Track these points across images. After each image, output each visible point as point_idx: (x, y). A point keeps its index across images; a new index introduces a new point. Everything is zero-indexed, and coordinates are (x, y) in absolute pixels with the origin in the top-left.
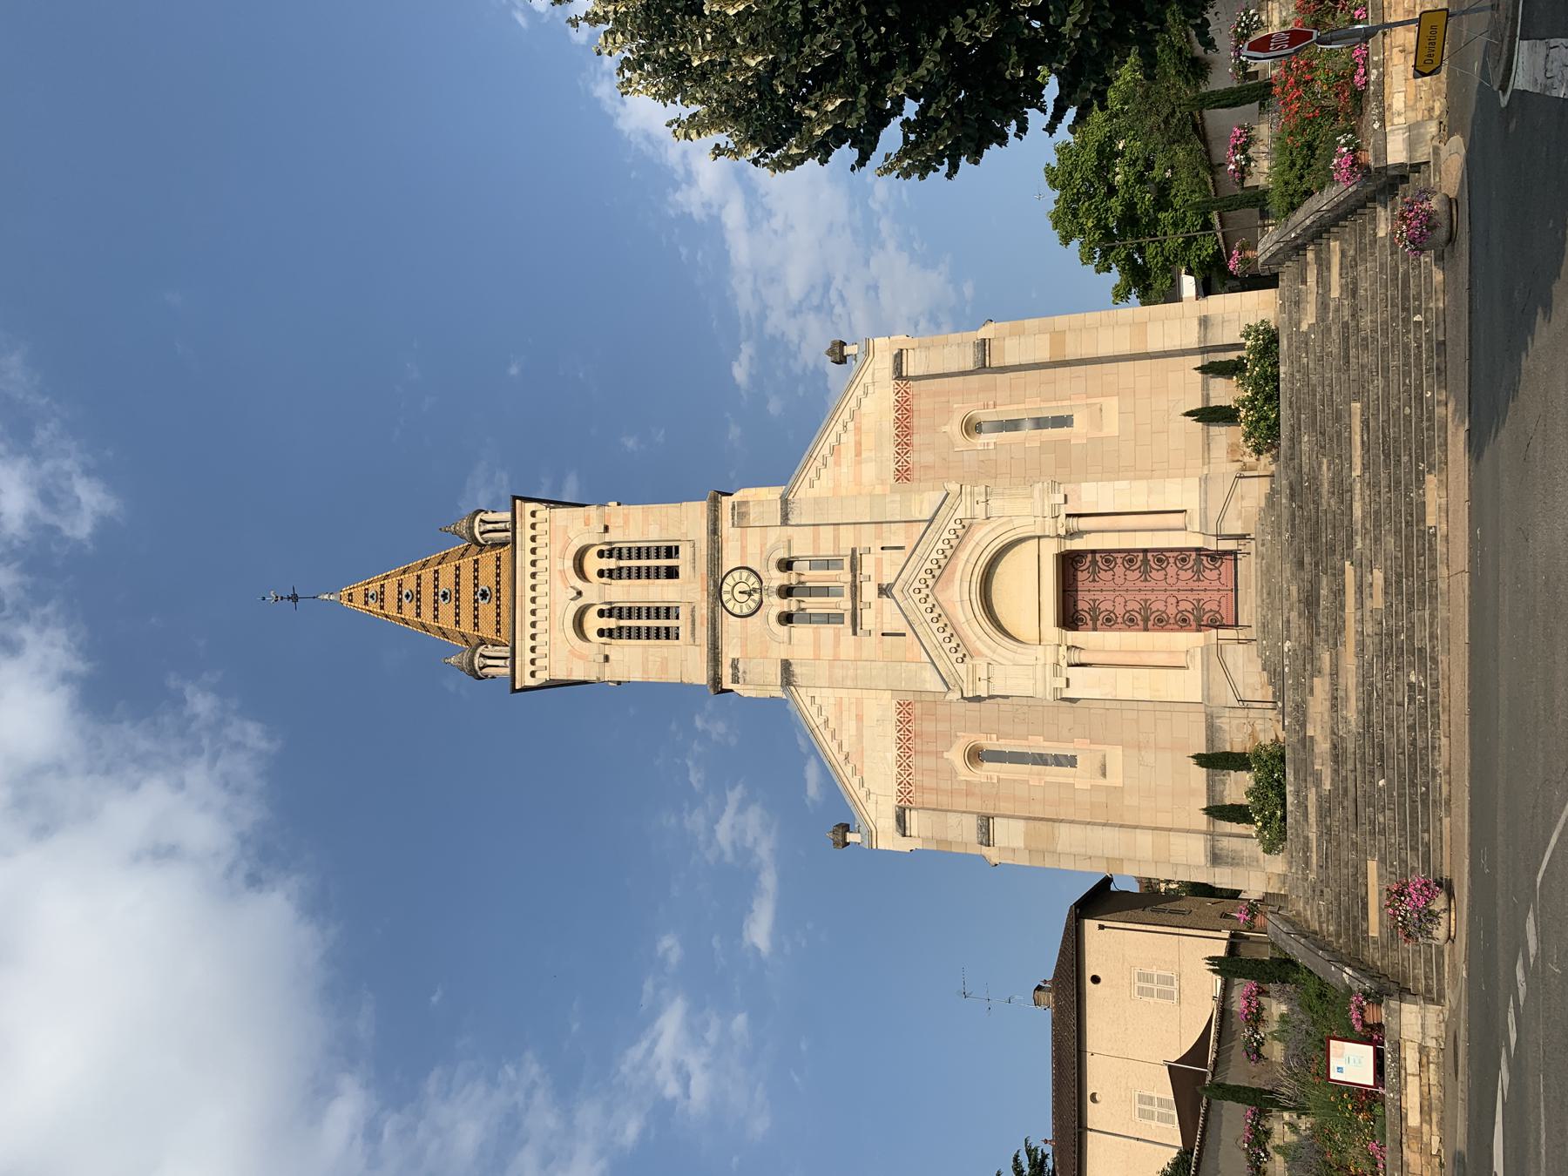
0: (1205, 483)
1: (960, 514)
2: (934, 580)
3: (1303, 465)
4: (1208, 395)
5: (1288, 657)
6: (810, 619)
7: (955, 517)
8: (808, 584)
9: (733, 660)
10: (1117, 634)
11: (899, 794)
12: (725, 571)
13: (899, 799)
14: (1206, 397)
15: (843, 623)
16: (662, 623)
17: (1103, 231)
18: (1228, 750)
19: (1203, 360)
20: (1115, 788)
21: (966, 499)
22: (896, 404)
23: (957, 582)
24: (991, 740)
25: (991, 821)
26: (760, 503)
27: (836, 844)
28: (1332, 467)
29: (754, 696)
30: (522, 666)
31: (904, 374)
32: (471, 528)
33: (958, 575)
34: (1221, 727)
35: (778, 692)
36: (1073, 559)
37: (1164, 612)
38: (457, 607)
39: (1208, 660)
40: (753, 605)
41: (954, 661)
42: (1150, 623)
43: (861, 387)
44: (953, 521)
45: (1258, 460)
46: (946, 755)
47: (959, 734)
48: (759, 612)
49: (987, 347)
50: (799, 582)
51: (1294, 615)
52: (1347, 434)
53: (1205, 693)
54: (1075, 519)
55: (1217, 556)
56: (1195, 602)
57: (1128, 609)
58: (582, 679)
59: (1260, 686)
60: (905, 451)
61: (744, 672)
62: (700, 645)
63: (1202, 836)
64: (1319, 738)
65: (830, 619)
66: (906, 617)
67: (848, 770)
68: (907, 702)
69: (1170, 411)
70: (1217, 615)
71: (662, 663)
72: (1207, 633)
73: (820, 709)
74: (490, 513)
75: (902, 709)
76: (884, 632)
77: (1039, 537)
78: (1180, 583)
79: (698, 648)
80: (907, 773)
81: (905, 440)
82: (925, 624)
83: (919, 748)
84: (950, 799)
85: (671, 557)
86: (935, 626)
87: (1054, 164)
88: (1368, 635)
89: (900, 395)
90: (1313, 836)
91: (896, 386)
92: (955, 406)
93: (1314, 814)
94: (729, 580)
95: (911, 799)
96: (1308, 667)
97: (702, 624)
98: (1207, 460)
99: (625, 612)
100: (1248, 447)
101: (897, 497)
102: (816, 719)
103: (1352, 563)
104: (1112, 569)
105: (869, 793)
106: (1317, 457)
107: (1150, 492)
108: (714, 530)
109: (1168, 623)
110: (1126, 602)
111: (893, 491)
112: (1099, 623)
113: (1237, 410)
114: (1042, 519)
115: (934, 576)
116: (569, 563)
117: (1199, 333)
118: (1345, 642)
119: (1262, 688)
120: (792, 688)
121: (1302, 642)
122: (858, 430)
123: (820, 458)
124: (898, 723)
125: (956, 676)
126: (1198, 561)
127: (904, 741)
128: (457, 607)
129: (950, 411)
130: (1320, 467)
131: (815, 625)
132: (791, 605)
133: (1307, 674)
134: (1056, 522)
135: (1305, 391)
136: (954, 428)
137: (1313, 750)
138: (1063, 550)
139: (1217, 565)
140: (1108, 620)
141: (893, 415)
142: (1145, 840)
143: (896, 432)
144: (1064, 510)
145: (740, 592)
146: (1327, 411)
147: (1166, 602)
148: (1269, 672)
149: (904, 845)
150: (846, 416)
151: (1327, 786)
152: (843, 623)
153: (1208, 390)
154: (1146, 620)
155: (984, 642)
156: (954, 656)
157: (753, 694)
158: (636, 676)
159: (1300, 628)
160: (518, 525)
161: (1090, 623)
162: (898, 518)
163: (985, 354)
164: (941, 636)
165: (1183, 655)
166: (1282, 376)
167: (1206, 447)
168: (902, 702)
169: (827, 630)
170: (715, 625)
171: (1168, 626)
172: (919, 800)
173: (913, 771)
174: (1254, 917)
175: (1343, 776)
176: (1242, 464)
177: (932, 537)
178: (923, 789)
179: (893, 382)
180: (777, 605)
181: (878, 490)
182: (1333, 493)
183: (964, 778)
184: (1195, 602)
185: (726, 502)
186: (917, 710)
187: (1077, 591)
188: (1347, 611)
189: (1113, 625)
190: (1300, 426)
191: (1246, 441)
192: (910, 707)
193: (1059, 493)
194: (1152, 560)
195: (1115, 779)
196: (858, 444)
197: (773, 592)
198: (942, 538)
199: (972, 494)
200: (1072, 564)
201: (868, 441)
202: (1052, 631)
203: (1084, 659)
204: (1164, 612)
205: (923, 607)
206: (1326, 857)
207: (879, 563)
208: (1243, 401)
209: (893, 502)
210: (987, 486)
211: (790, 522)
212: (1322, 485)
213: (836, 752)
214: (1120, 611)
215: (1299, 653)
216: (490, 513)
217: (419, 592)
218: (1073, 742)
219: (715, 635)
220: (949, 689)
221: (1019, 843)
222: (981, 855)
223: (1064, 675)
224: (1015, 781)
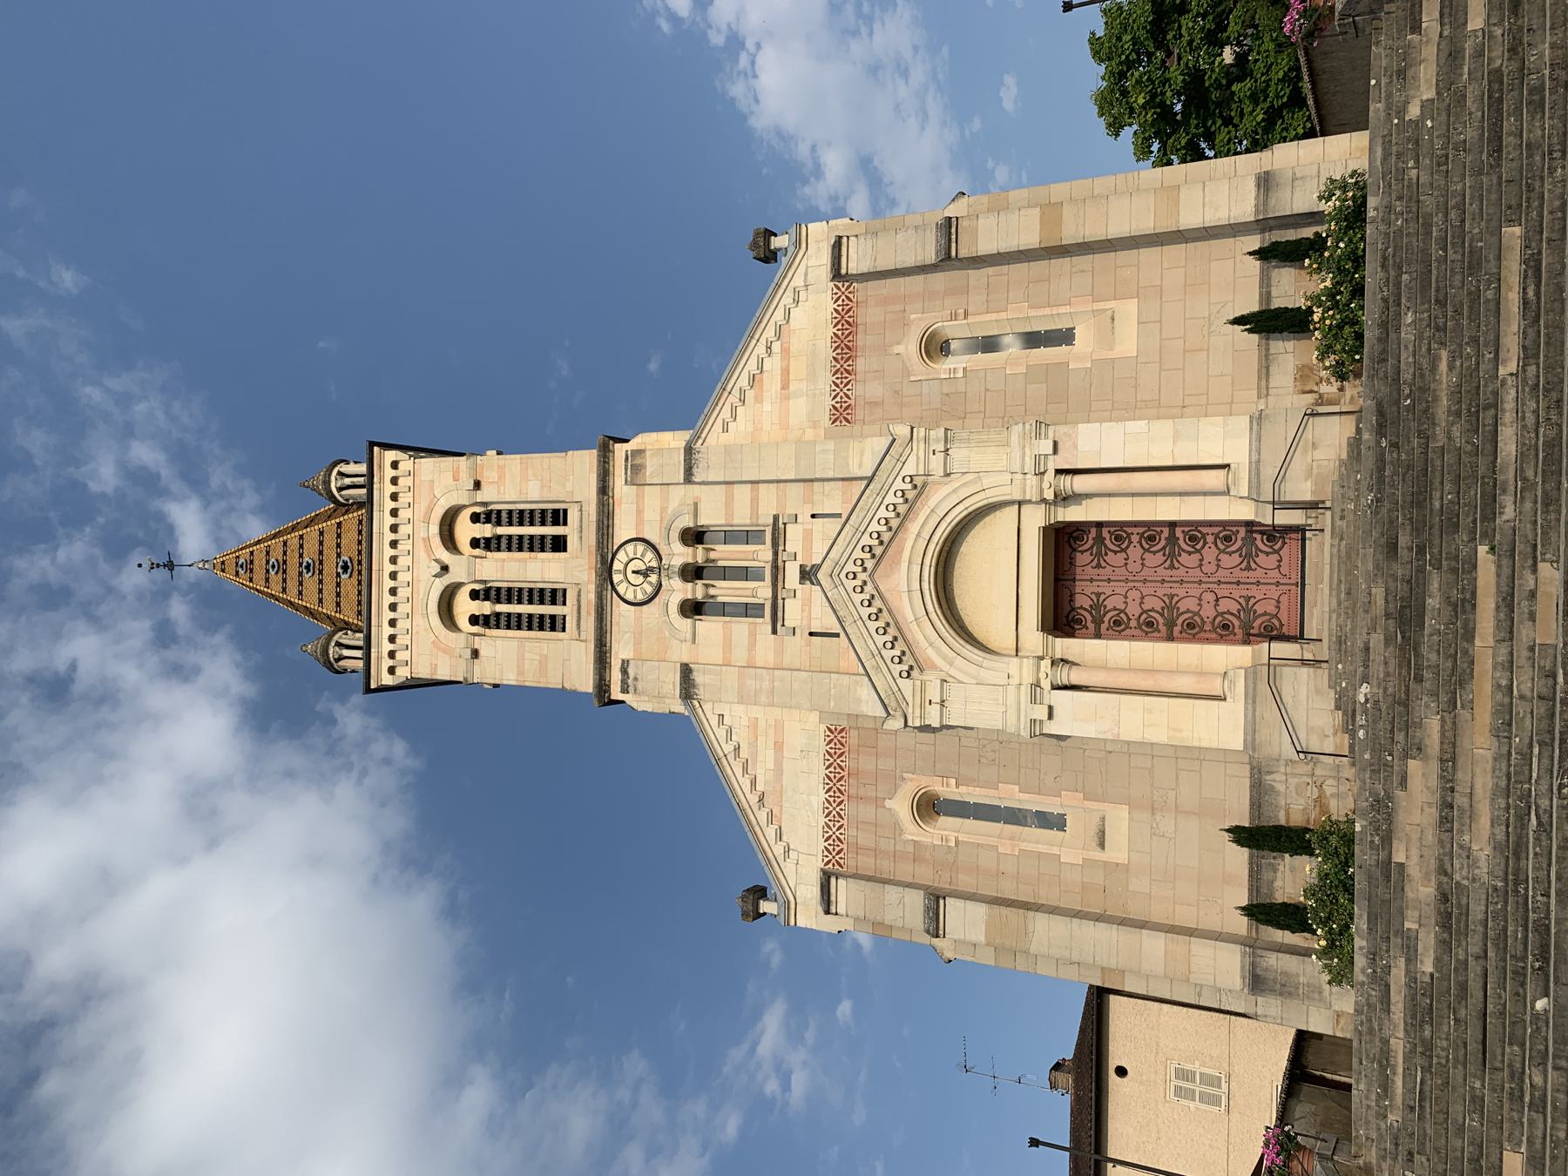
0: (1259, 424)
1: (909, 469)
2: (874, 561)
3: (1403, 366)
4: (1269, 293)
5: (1365, 712)
6: (723, 610)
7: (903, 473)
8: (720, 563)
9: (623, 661)
10: (1126, 643)
11: (826, 853)
12: (617, 542)
13: (826, 860)
14: (1266, 296)
15: (763, 617)
16: (547, 610)
17: (1159, 110)
18: (1283, 822)
19: (1263, 240)
20: (1117, 864)
21: (919, 448)
23: (904, 565)
24: (948, 785)
25: (941, 902)
26: (660, 451)
27: (745, 915)
28: (1458, 363)
29: (650, 710)
30: (379, 659)
31: (843, 271)
32: (327, 483)
33: (906, 554)
34: (1272, 787)
35: (679, 707)
36: (1070, 535)
37: (1197, 614)
38: (321, 582)
39: (1255, 689)
40: (649, 589)
41: (896, 675)
42: (1177, 629)
43: (789, 293)
44: (900, 478)
45: (1341, 389)
46: (888, 803)
48: (657, 600)
49: (953, 230)
50: (708, 560)
51: (1377, 640)
52: (1490, 294)
53: (1249, 738)
54: (1069, 478)
55: (1275, 534)
56: (1242, 601)
57: (1146, 607)
58: (448, 678)
59: (1332, 731)
60: (845, 381)
61: (636, 679)
62: (586, 641)
63: (1239, 947)
64: (1414, 870)
65: (749, 610)
66: (835, 611)
67: (762, 816)
68: (839, 728)
69: (1212, 318)
71: (540, 661)
72: (1256, 647)
73: (730, 731)
74: (352, 464)
75: (832, 736)
77: (1020, 503)
78: (1221, 572)
79: (583, 644)
80: (838, 825)
81: (845, 366)
82: (860, 623)
83: (853, 791)
84: (892, 864)
85: (559, 525)
86: (873, 625)
87: (1100, 33)
88: (1522, 697)
90: (1398, 1046)
92: (913, 316)
93: (1401, 1006)
94: (621, 556)
95: (842, 862)
96: (1400, 737)
97: (589, 613)
98: (1264, 391)
99: (503, 594)
100: (1326, 368)
101: (831, 445)
103: (1492, 549)
104: (1124, 550)
105: (787, 850)
106: (1429, 350)
107: (1177, 437)
108: (604, 489)
109: (1202, 630)
110: (1143, 598)
111: (828, 436)
112: (1104, 626)
113: (1310, 311)
114: (1020, 476)
115: (873, 556)
116: (434, 529)
117: (1257, 198)
118: (1472, 701)
119: (1335, 734)
120: (695, 703)
121: (1390, 690)
122: (786, 352)
123: (736, 392)
124: (827, 757)
125: (898, 695)
126: (1250, 539)
127: (835, 781)
128: (321, 582)
129: (906, 324)
130: (1434, 368)
131: (728, 619)
132: (697, 591)
133: (1398, 748)
134: (1042, 481)
135: (1411, 230)
136: (909, 348)
137: (1403, 890)
138: (1052, 522)
139: (1276, 547)
140: (1117, 623)
141: (831, 330)
142: (1154, 946)
143: (834, 354)
145: (634, 572)
146: (1451, 254)
148: (1345, 713)
149: (829, 925)
150: (770, 333)
151: (1427, 966)
152: (763, 617)
153: (1269, 286)
154: (1171, 624)
155: (938, 651)
156: (896, 669)
157: (648, 707)
158: (510, 678)
159: (1386, 663)
160: (376, 480)
161: (1091, 626)
162: (830, 475)
163: (950, 239)
165: (1219, 680)
166: (1371, 213)
167: (1264, 371)
168: (833, 728)
169: (741, 626)
171: (1202, 635)
172: (852, 863)
173: (845, 822)
174: (1289, 1157)
175: (1457, 960)
176: (1317, 396)
177: (871, 501)
178: (858, 849)
180: (679, 590)
181: (810, 434)
182: (1458, 414)
183: (911, 838)
184: (1242, 601)
185: (620, 450)
186: (853, 739)
187: (1074, 580)
188: (1478, 642)
189: (1123, 630)
190: (1399, 296)
191: (1321, 359)
192: (843, 734)
193: (1046, 437)
194: (1108, 539)
195: (1117, 850)
196: (786, 372)
197: (674, 573)
198: (886, 502)
199: (926, 440)
200: (1069, 542)
201: (798, 368)
202: (1033, 637)
203: (1076, 677)
204: (1197, 614)
205: (858, 598)
206: (1417, 1105)
207: (808, 536)
208: (1318, 296)
209: (825, 451)
210: (946, 429)
211: (694, 479)
212: (1436, 399)
214: (1134, 610)
215: (1384, 708)
216: (352, 464)
217: (285, 562)
218: (1060, 796)
220: (889, 714)
221: (979, 936)
223: (1046, 702)
224: (978, 844)
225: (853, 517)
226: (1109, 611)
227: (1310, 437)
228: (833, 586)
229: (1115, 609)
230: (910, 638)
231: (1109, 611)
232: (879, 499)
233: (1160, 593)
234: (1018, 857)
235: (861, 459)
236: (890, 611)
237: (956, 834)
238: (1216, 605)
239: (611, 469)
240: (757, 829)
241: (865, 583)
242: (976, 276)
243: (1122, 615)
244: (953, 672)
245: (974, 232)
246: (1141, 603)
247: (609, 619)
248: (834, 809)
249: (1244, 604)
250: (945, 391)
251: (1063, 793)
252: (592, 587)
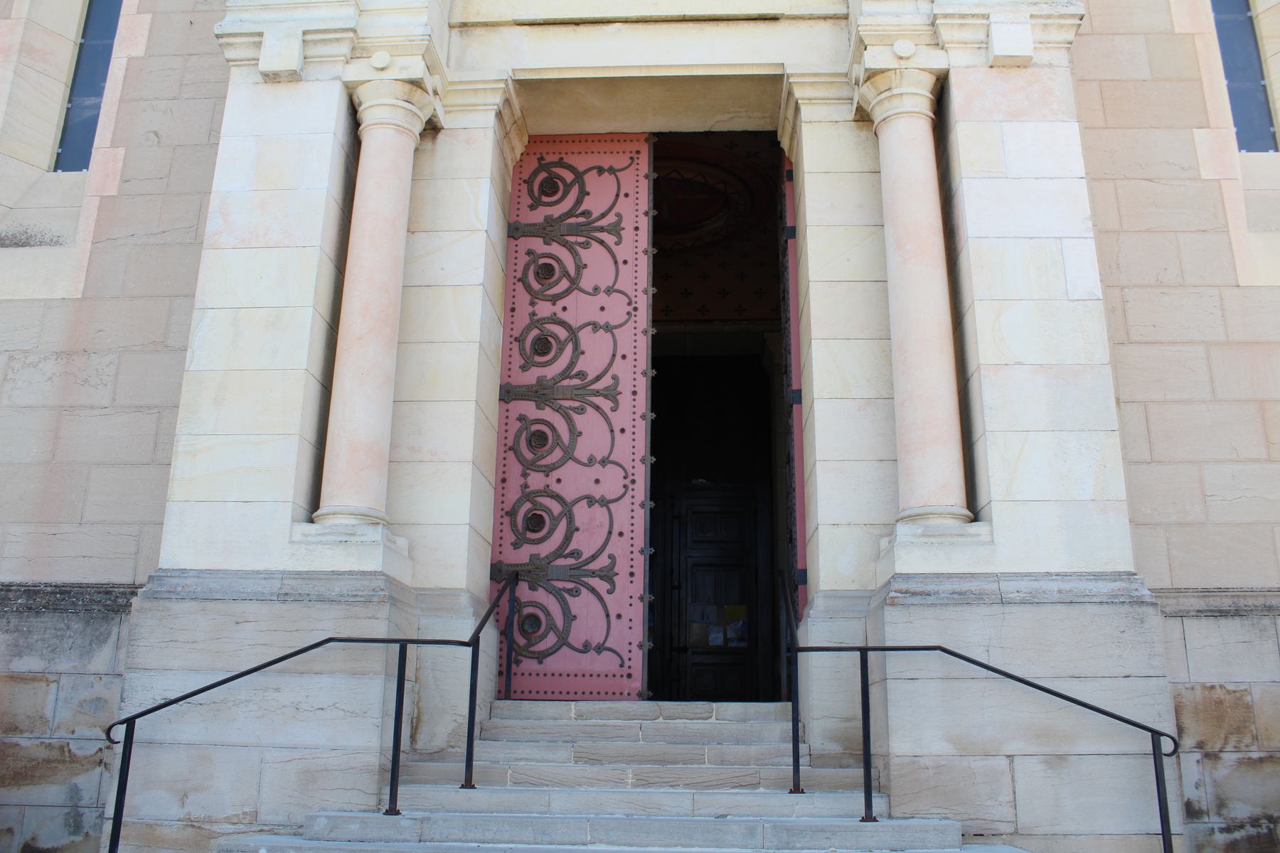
37: (569, 456)
57: (585, 336)
59: (198, 813)
70: (551, 639)
109: (528, 467)
119: (191, 823)
144: (957, 61)
147: (604, 462)
154: (542, 394)
167: (1226, 603)
171: (516, 468)
189: (528, 288)
204: (569, 456)
226: (575, 254)
227: (1083, 748)
229: (580, 267)
231: (575, 254)
233: (619, 368)
238: (591, 501)
243: (565, 284)
246: (595, 326)
249: (594, 566)
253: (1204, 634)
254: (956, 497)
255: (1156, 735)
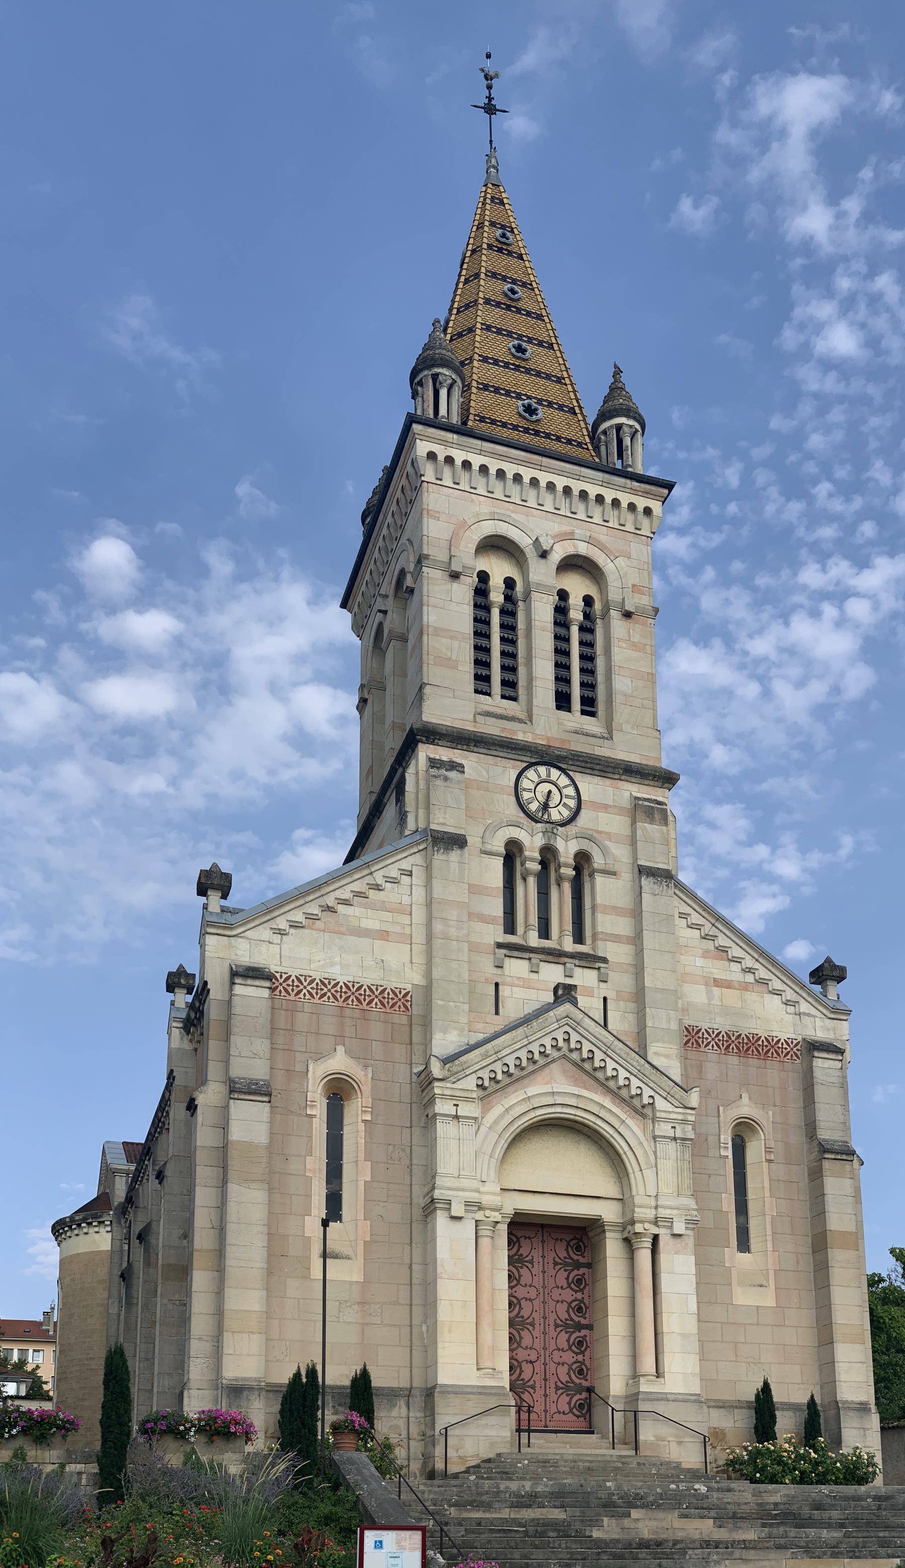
0: (695, 1401)
1: (660, 1104)
7: (657, 1097)
20: (309, 1269)
21: (678, 1114)
22: (775, 1039)
23: (576, 1090)
25: (266, 1099)
41: (480, 1074)
44: (653, 1093)
46: (341, 1049)
47: (370, 1070)
49: (844, 1157)
61: (446, 779)
73: (395, 881)
76: (500, 987)
79: (471, 717)
80: (314, 992)
82: (525, 1042)
83: (347, 1012)
86: (523, 1054)
89: (785, 1046)
91: (795, 1042)
94: (564, 781)
97: (503, 730)
101: (674, 1026)
102: (381, 873)
105: (281, 933)
124: (380, 989)
125: (461, 1075)
129: (764, 1106)
136: (746, 1108)
144: (663, 1232)
145: (550, 792)
155: (501, 1116)
156: (485, 1074)
163: (838, 1153)
164: (511, 1061)
167: (721, 1404)
168: (408, 998)
170: (508, 747)
173: (316, 1001)
177: (635, 1063)
179: (800, 1039)
183: (311, 1068)
192: (403, 1009)
199: (684, 1122)
213: (339, 894)
219: (494, 744)
222: (206, 1080)
225: (620, 1045)
228: (559, 1017)
230: (510, 1089)
232: (635, 1071)
234: (304, 1175)
235: (662, 1055)
236: (533, 1072)
237: (318, 1116)
239: (647, 782)
240: (301, 902)
241: (559, 1049)
242: (800, 1173)
244: (483, 1129)
245: (841, 1175)
247: (501, 754)
248: (329, 991)
250: (710, 1138)
251: (369, 1222)
252: (529, 738)
253: (714, 1413)
254: (653, 1371)
255: (705, 1436)
